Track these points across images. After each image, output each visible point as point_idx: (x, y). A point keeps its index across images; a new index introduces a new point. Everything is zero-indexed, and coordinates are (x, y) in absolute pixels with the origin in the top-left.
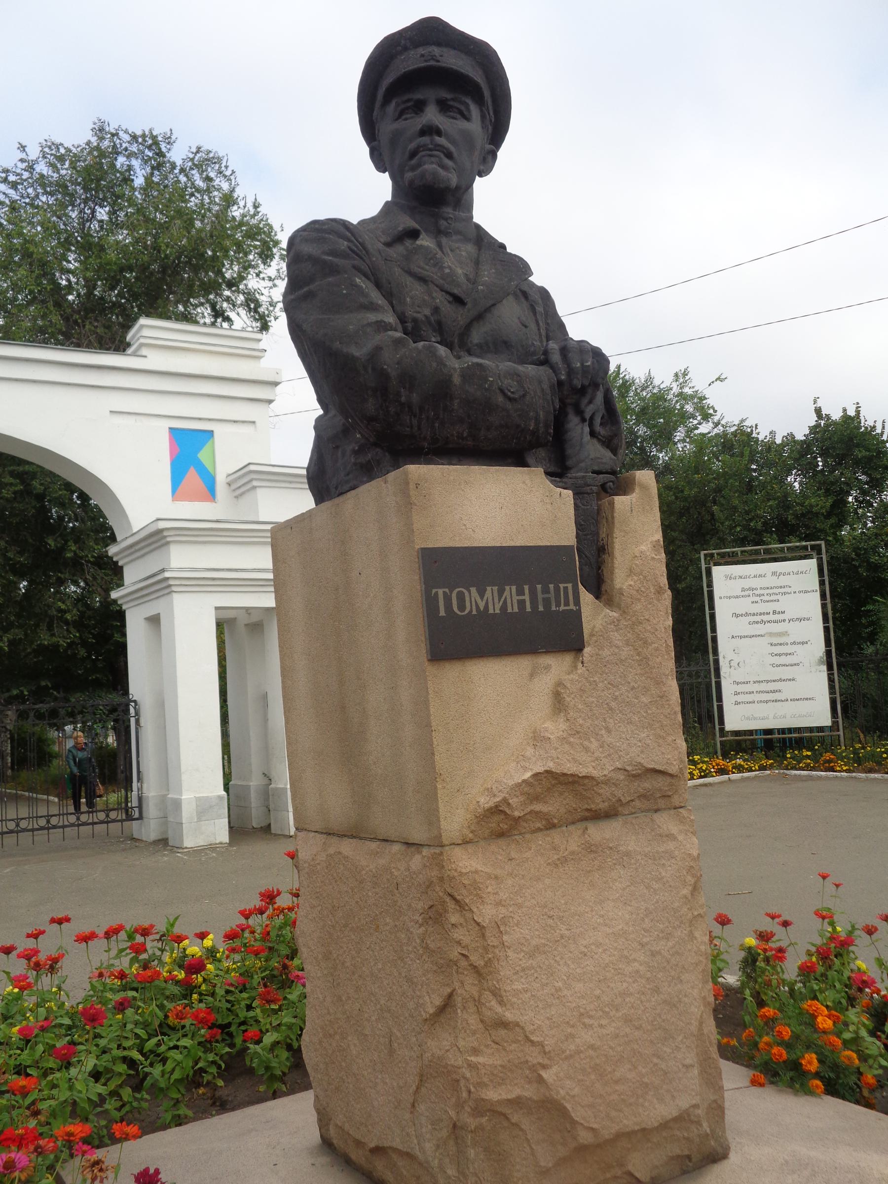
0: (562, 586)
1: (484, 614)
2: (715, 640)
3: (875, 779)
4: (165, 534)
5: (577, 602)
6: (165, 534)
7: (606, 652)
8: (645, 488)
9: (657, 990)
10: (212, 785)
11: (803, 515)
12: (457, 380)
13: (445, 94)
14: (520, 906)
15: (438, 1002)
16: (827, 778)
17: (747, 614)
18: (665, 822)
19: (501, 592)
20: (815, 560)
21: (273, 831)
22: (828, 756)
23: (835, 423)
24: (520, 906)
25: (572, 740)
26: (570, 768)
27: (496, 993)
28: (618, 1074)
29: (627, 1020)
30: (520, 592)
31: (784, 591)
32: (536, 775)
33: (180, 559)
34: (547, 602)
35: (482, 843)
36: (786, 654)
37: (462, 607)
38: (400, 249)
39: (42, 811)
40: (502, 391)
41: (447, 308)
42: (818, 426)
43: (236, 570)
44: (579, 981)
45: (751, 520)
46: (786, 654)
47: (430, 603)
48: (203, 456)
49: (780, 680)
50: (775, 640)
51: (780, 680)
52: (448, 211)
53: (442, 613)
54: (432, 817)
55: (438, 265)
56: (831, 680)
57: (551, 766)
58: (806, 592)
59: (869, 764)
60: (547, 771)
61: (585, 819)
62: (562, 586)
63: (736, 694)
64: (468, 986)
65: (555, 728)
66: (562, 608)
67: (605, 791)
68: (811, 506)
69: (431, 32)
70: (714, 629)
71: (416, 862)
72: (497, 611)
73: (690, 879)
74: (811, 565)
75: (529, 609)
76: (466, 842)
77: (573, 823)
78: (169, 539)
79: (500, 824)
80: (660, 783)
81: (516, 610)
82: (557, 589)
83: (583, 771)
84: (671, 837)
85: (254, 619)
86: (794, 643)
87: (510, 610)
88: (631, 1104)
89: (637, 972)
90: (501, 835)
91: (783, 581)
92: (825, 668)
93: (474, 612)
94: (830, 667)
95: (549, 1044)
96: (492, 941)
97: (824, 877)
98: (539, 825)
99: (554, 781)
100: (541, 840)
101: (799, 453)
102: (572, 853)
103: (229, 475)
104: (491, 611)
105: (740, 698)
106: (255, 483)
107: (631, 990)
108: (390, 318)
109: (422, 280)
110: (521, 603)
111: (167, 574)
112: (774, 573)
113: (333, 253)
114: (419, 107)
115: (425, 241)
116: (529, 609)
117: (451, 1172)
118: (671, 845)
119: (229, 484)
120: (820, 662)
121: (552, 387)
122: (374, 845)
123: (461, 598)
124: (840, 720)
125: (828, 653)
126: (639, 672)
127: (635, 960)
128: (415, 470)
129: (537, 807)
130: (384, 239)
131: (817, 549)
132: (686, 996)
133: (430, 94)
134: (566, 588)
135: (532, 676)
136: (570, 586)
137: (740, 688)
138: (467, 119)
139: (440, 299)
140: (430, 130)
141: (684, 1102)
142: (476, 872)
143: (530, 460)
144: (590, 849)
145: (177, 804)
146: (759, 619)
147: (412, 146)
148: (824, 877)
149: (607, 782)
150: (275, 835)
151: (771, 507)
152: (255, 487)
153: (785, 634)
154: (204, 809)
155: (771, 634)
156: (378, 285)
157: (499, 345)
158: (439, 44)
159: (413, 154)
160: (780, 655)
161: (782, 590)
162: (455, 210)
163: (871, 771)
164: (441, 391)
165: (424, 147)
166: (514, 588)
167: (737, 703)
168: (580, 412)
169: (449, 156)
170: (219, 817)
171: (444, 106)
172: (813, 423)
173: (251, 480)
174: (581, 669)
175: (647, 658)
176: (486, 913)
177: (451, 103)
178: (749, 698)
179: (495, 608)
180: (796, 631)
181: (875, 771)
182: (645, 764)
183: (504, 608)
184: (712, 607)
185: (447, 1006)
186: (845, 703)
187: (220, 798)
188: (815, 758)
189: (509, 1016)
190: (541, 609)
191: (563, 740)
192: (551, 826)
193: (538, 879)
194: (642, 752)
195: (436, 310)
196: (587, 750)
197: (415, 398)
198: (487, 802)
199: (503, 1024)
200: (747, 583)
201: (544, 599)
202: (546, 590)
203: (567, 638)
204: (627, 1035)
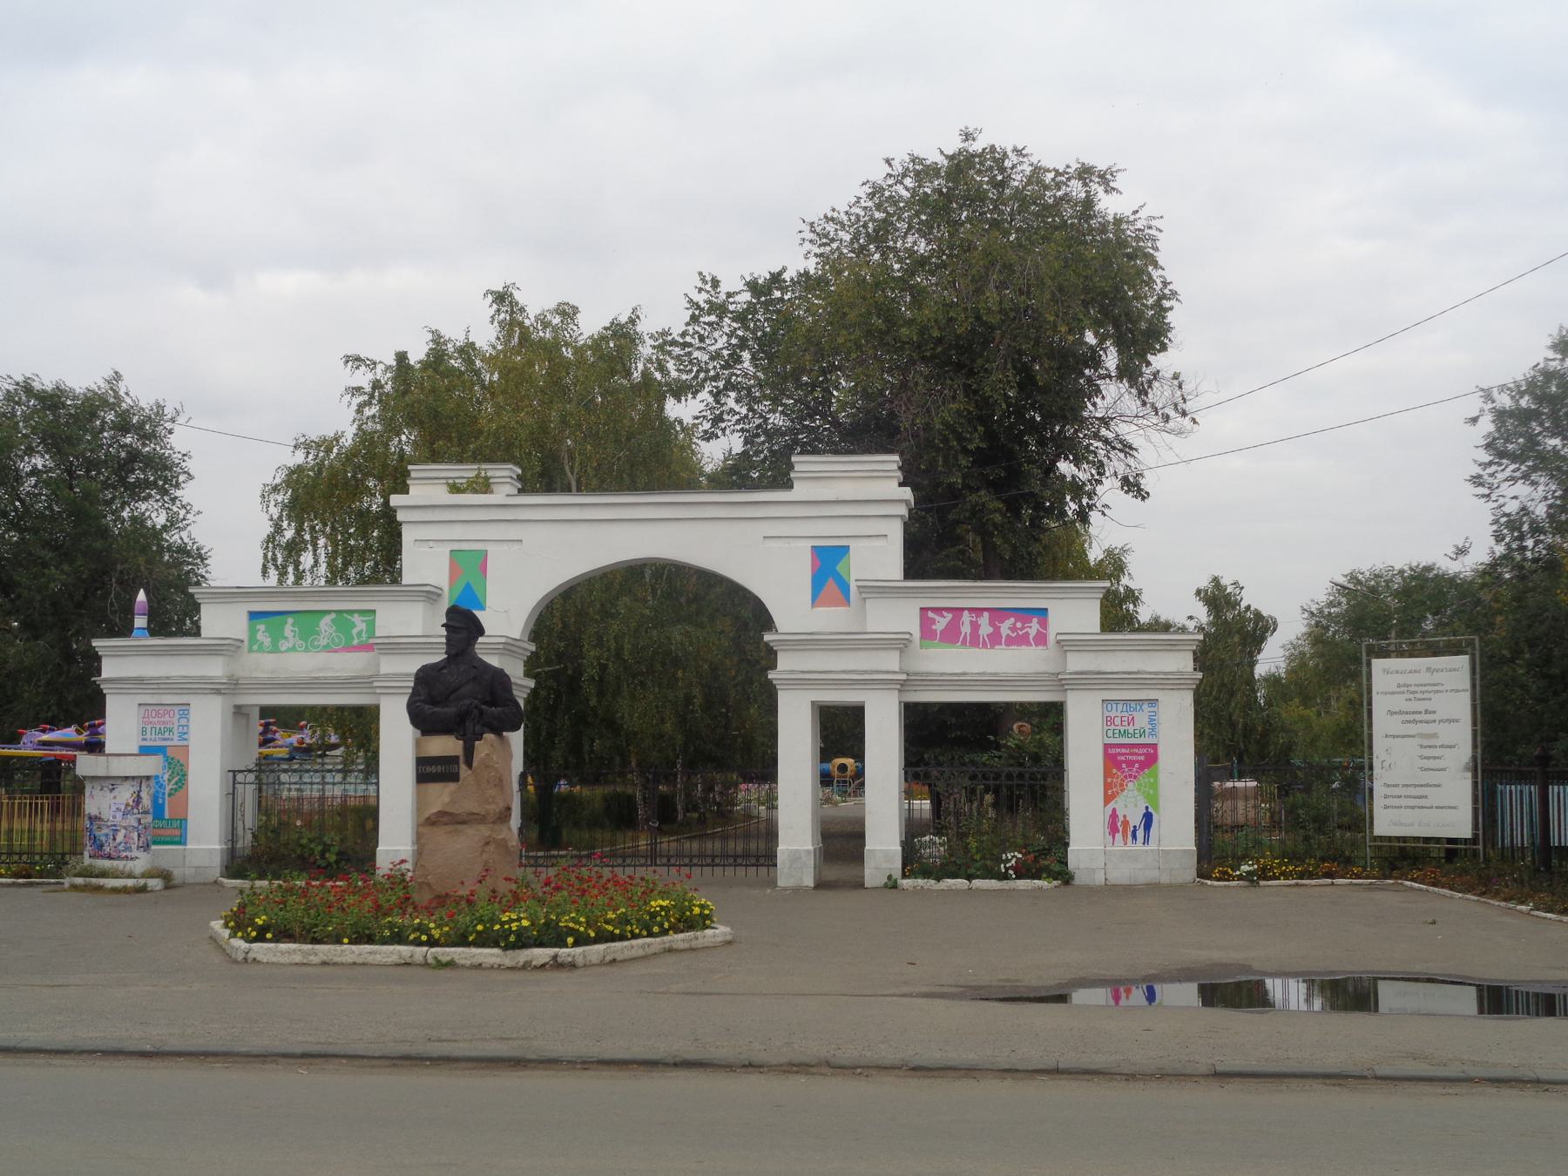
2: (1370, 736)
17: (1400, 713)
18: (482, 827)
31: (1436, 688)
49: (1427, 785)
50: (1426, 742)
51: (1427, 785)
63: (1386, 797)
70: (1370, 725)
74: (1463, 661)
91: (1437, 678)
92: (1469, 775)
94: (1475, 776)
105: (1389, 802)
112: (1428, 669)
120: (1466, 769)
125: (1474, 758)
131: (1471, 643)
137: (1389, 791)
146: (1411, 718)
153: (1435, 735)
154: (795, 856)
155: (1421, 735)
167: (1386, 807)
178: (1396, 802)
180: (1447, 733)
184: (1370, 703)
187: (808, 851)
200: (1402, 679)
203: (454, 778)
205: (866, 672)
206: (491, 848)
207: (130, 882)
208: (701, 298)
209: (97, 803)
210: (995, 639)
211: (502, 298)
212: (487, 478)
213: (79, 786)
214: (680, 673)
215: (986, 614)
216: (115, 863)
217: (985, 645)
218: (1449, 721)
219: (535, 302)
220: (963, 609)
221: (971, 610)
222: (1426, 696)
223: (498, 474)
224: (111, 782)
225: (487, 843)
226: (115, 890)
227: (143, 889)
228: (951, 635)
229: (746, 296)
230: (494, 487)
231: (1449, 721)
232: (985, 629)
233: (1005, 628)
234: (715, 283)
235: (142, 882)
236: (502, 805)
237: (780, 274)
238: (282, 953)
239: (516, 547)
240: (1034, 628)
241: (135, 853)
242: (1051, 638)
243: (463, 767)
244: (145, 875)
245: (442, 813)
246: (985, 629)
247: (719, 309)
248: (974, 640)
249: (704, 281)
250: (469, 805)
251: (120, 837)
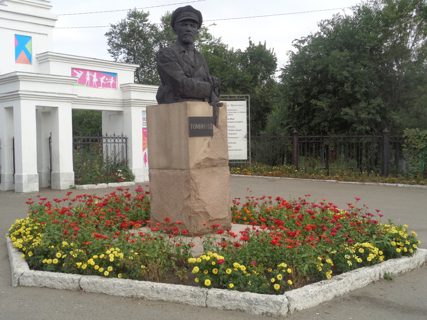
3: (260, 178)
4: (19, 77)
6: (19, 77)
9: (223, 196)
10: (34, 171)
11: (242, 81)
12: (196, 86)
13: (192, 24)
15: (187, 196)
16: (244, 177)
20: (246, 102)
21: (52, 188)
22: (245, 170)
23: (255, 47)
26: (211, 157)
27: (198, 194)
33: (24, 87)
34: (208, 127)
36: (234, 134)
38: (181, 54)
41: (191, 69)
42: (250, 48)
43: (44, 92)
45: (223, 82)
46: (234, 134)
47: (190, 127)
48: (27, 46)
52: (189, 45)
54: (188, 163)
55: (189, 59)
56: (248, 143)
57: (208, 156)
58: (242, 112)
59: (259, 173)
64: (193, 193)
65: (208, 150)
67: (216, 162)
68: (245, 78)
69: (189, 9)
71: (183, 172)
74: (245, 103)
76: (193, 169)
78: (20, 79)
79: (199, 166)
80: (224, 161)
83: (213, 158)
84: (226, 171)
85: (46, 110)
86: (237, 130)
90: (199, 168)
91: (235, 108)
92: (246, 139)
94: (248, 139)
95: (206, 203)
96: (198, 186)
97: (248, 189)
99: (209, 159)
101: (242, 57)
103: (37, 55)
106: (49, 59)
108: (183, 72)
109: (186, 62)
111: (19, 93)
112: (232, 105)
113: (171, 57)
114: (186, 25)
115: (186, 54)
117: (188, 224)
119: (37, 58)
120: (245, 137)
122: (173, 170)
123: (194, 126)
124: (250, 158)
125: (248, 134)
128: (188, 102)
129: (205, 164)
130: (179, 52)
131: (247, 97)
133: (189, 23)
139: (190, 67)
140: (188, 31)
141: (226, 216)
143: (205, 100)
144: (213, 172)
145: (20, 177)
147: (185, 33)
148: (248, 189)
150: (53, 190)
151: (231, 77)
152: (49, 61)
153: (234, 127)
154: (30, 179)
156: (179, 64)
157: (199, 75)
158: (191, 12)
159: (185, 35)
160: (232, 134)
161: (234, 111)
163: (258, 175)
164: (193, 88)
165: (187, 34)
168: (214, 91)
169: (192, 36)
170: (36, 182)
171: (191, 25)
172: (248, 47)
173: (48, 58)
174: (213, 140)
176: (197, 181)
179: (200, 128)
181: (260, 175)
185: (189, 196)
186: (252, 152)
187: (36, 175)
188: (241, 170)
189: (200, 198)
192: (206, 167)
195: (189, 69)
198: (197, 162)
199: (199, 199)
205: (50, 93)
210: (99, 84)
215: (95, 73)
217: (95, 87)
218: (239, 122)
220: (87, 70)
221: (90, 71)
222: (231, 114)
228: (82, 81)
231: (239, 122)
232: (95, 80)
233: (102, 79)
238: (312, 297)
240: (112, 81)
242: (118, 86)
246: (95, 80)
248: (91, 84)
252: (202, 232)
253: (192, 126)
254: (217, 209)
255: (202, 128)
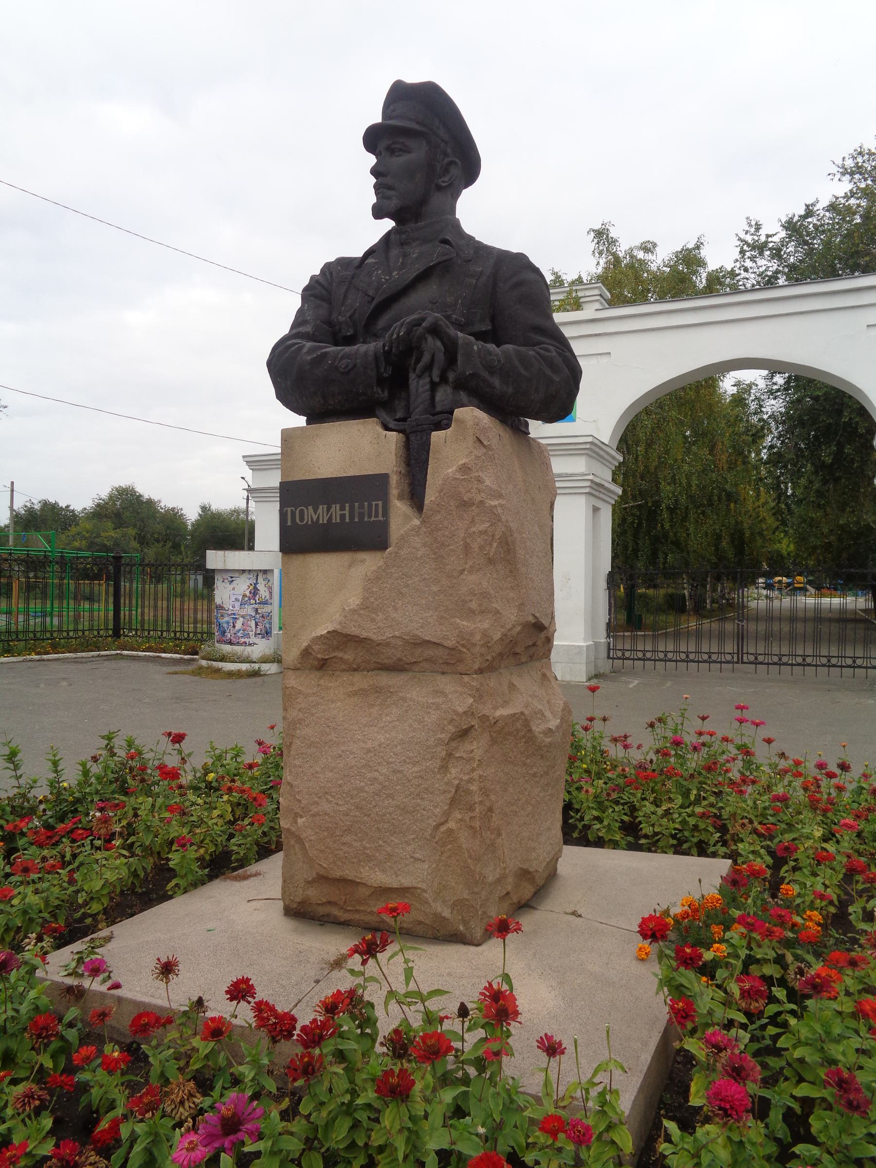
0: (374, 503)
1: (315, 524)
5: (386, 513)
7: (403, 553)
8: (461, 422)
14: (313, 715)
18: (447, 684)
19: (328, 510)
24: (313, 715)
25: (362, 612)
26: (354, 630)
28: (345, 839)
29: (358, 808)
30: (342, 508)
32: (329, 632)
34: (361, 515)
35: (307, 671)
37: (302, 519)
39: (775, 650)
40: (336, 368)
44: (331, 771)
53: (289, 523)
57: (338, 627)
60: (334, 631)
61: (379, 669)
62: (374, 503)
66: (373, 519)
72: (325, 522)
73: (451, 729)
75: (347, 520)
76: (296, 669)
77: (373, 670)
81: (338, 521)
82: (370, 506)
83: (364, 634)
87: (334, 521)
88: (353, 863)
89: (376, 779)
93: (310, 523)
98: (344, 667)
100: (346, 677)
102: (363, 690)
104: (321, 522)
107: (367, 788)
110: (343, 516)
116: (347, 520)
118: (440, 700)
121: (376, 358)
123: (302, 513)
126: (434, 566)
127: (377, 770)
129: (340, 654)
132: (424, 810)
134: (377, 505)
135: (350, 566)
136: (380, 503)
138: (409, 152)
141: (406, 882)
142: (293, 688)
149: (387, 645)
162: (416, 222)
166: (338, 506)
175: (442, 557)
177: (393, 146)
182: (423, 637)
183: (330, 519)
190: (356, 520)
191: (354, 611)
193: (333, 702)
194: (422, 627)
196: (373, 620)
197: (289, 383)
201: (359, 513)
202: (361, 507)
204: (355, 816)
206: (476, 747)
207: (244, 667)
208: (749, 238)
209: (227, 594)
211: (601, 234)
212: (578, 298)
213: (209, 578)
214: (732, 505)
216: (235, 648)
219: (626, 241)
223: (588, 293)
224: (232, 574)
225: (463, 734)
226: (231, 674)
227: (256, 674)
229: (783, 234)
230: (584, 306)
234: (758, 227)
235: (256, 666)
236: (511, 617)
237: (813, 205)
239: (604, 360)
241: (253, 639)
243: (399, 507)
244: (264, 660)
245: (340, 639)
247: (760, 248)
249: (750, 225)
250: (412, 617)
251: (239, 625)
252: (322, 911)
253: (293, 514)
254: (347, 839)
255: (336, 519)
